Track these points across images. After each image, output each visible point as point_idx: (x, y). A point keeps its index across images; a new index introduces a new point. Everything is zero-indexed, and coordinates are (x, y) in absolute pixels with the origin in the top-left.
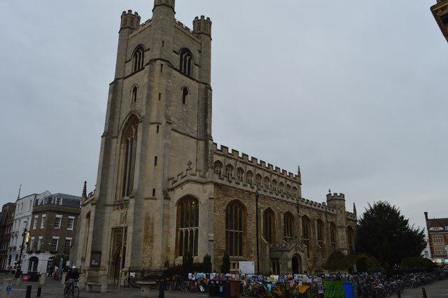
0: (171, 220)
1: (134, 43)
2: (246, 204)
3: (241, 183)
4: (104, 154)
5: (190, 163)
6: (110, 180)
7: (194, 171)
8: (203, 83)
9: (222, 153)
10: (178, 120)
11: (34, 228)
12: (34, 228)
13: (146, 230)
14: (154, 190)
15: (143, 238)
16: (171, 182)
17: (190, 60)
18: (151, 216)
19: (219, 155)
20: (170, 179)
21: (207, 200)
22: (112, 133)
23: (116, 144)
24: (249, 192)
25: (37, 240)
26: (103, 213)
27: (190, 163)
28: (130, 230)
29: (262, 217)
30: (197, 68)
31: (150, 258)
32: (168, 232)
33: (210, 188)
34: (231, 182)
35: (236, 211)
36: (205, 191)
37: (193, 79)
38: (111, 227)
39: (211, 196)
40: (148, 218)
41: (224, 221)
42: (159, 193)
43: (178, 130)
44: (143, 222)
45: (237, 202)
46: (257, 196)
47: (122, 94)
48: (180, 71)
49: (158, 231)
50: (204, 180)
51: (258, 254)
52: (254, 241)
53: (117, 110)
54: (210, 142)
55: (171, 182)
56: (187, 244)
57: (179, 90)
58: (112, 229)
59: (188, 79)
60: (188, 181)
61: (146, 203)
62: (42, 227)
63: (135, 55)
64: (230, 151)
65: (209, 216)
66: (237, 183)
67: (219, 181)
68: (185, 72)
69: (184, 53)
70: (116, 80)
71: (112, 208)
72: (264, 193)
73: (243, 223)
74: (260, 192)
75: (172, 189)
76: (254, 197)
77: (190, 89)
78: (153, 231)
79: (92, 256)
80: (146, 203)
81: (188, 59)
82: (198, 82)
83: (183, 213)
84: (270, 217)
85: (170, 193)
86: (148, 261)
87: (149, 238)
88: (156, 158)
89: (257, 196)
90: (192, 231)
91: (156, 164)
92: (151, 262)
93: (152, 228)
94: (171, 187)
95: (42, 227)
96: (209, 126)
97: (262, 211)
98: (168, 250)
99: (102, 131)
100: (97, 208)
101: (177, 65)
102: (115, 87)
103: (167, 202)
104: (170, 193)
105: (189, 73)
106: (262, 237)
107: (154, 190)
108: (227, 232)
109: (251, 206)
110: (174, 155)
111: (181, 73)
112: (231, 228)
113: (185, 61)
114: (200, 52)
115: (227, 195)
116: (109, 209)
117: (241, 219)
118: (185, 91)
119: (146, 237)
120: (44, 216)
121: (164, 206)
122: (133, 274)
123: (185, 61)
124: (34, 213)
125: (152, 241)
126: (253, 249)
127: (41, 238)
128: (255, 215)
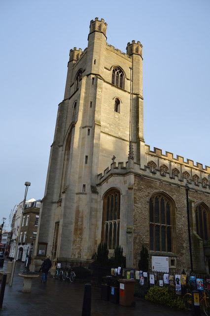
0: (98, 213)
1: (76, 69)
2: (174, 197)
3: (167, 175)
4: (52, 160)
5: (114, 158)
6: (57, 182)
7: (117, 166)
8: (134, 94)
9: (155, 154)
10: (110, 125)
11: (23, 226)
12: (23, 226)
13: (76, 222)
14: (84, 186)
15: (73, 231)
16: (99, 177)
17: (121, 75)
18: (80, 209)
19: (152, 155)
20: (99, 175)
21: (127, 191)
22: (59, 143)
23: (61, 151)
24: (178, 185)
25: (23, 234)
26: (50, 210)
27: (114, 158)
28: (61, 223)
29: (193, 211)
30: (129, 81)
31: (79, 250)
32: (96, 225)
33: (132, 178)
34: (154, 173)
35: (163, 203)
36: (125, 182)
37: (125, 91)
38: (55, 222)
39: (130, 186)
40: (78, 212)
41: (147, 213)
42: (88, 188)
43: (110, 134)
44: (74, 216)
45: (163, 194)
46: (187, 189)
47: (67, 112)
48: (112, 84)
49: (86, 225)
50: (123, 171)
51: (190, 249)
52: (185, 236)
53: (64, 124)
54: (142, 143)
55: (99, 177)
56: (110, 235)
57: (111, 100)
58: (56, 223)
59: (120, 91)
60: (112, 175)
61: (76, 198)
62: (27, 225)
63: (77, 79)
64: (164, 153)
65: (128, 207)
66: (163, 175)
67: (141, 172)
68: (117, 86)
69: (116, 70)
70: (65, 100)
71: (56, 205)
72: (196, 187)
73: (171, 217)
74: (190, 186)
75: (100, 185)
76: (183, 191)
77: (121, 99)
78: (82, 224)
79: (38, 246)
80: (76, 198)
81: (120, 75)
82: (129, 93)
83: (108, 208)
84: (204, 212)
85: (98, 188)
86: (77, 253)
87: (79, 230)
88: (87, 157)
89: (187, 189)
90: (115, 224)
91: (86, 163)
92: (79, 253)
93: (82, 221)
94: (99, 182)
95: (27, 225)
96: (140, 130)
97: (193, 205)
98: (96, 243)
99: (52, 142)
100: (44, 205)
101: (110, 80)
102: (62, 106)
103: (94, 196)
104: (98, 188)
105: (121, 86)
106: (195, 232)
107: (84, 186)
108: (151, 226)
109: (181, 201)
110: (105, 155)
111: (118, 88)
112: (158, 221)
113: (117, 77)
114: (131, 69)
115: (151, 187)
116: (55, 206)
117: (168, 213)
118: (118, 102)
119: (76, 230)
120: (28, 216)
121: (91, 200)
122: (59, 265)
123: (117, 77)
124: (24, 214)
125: (81, 234)
126: (185, 245)
127: (25, 233)
128: (186, 209)
